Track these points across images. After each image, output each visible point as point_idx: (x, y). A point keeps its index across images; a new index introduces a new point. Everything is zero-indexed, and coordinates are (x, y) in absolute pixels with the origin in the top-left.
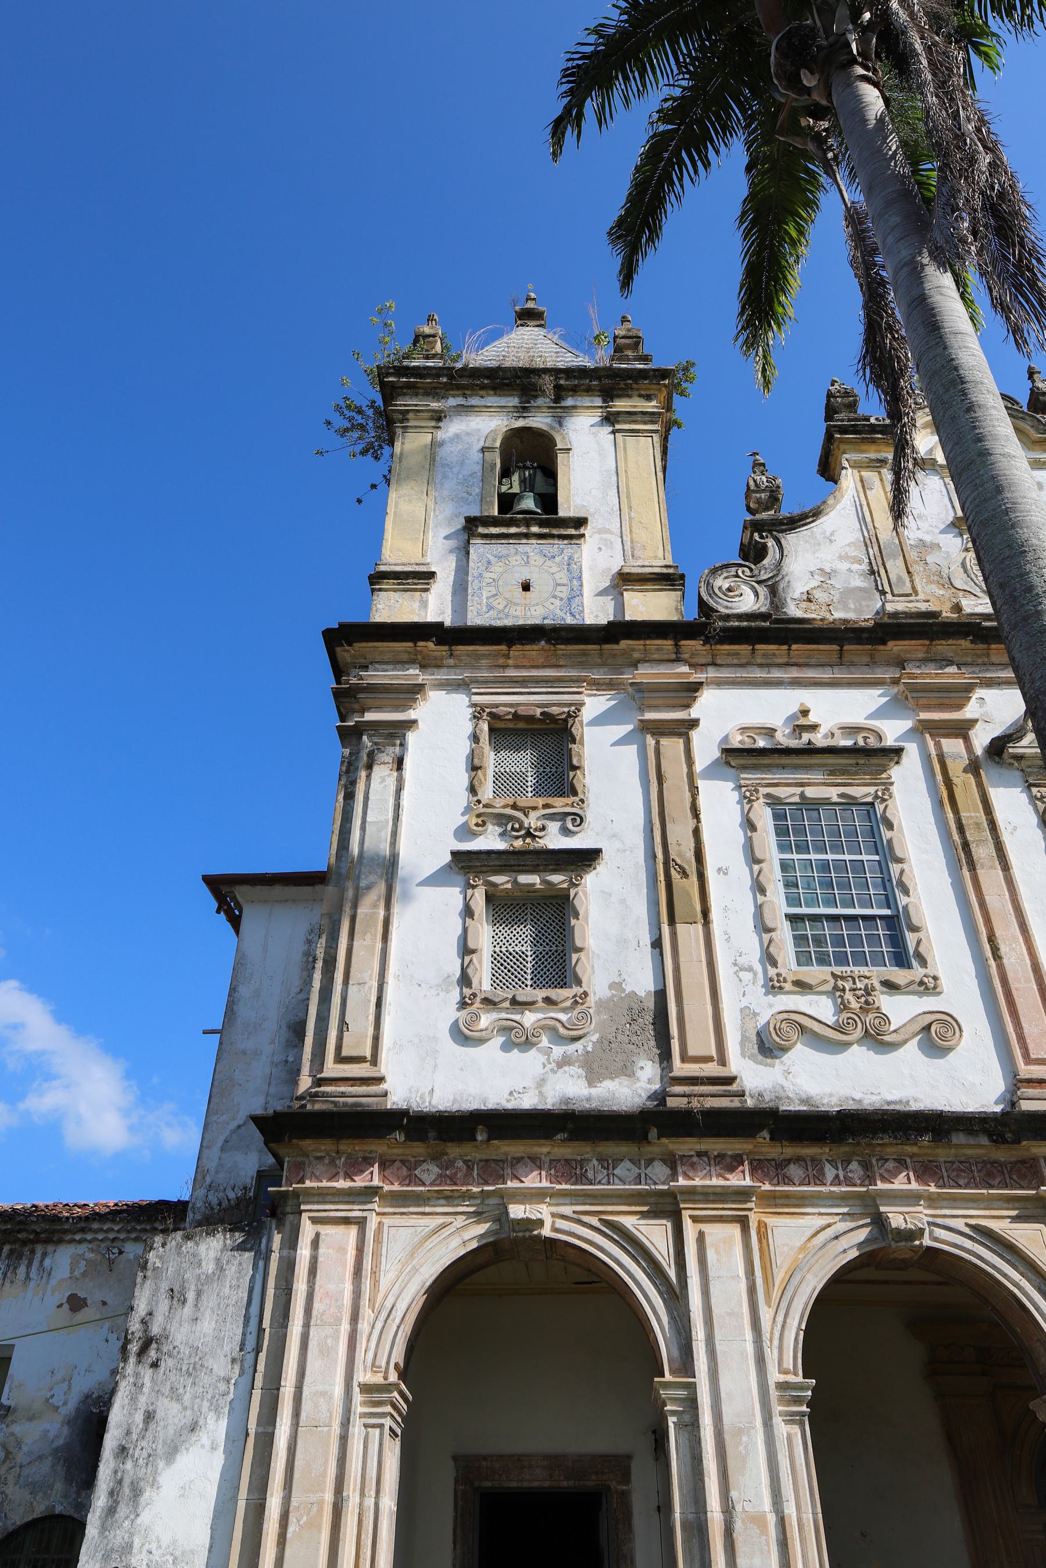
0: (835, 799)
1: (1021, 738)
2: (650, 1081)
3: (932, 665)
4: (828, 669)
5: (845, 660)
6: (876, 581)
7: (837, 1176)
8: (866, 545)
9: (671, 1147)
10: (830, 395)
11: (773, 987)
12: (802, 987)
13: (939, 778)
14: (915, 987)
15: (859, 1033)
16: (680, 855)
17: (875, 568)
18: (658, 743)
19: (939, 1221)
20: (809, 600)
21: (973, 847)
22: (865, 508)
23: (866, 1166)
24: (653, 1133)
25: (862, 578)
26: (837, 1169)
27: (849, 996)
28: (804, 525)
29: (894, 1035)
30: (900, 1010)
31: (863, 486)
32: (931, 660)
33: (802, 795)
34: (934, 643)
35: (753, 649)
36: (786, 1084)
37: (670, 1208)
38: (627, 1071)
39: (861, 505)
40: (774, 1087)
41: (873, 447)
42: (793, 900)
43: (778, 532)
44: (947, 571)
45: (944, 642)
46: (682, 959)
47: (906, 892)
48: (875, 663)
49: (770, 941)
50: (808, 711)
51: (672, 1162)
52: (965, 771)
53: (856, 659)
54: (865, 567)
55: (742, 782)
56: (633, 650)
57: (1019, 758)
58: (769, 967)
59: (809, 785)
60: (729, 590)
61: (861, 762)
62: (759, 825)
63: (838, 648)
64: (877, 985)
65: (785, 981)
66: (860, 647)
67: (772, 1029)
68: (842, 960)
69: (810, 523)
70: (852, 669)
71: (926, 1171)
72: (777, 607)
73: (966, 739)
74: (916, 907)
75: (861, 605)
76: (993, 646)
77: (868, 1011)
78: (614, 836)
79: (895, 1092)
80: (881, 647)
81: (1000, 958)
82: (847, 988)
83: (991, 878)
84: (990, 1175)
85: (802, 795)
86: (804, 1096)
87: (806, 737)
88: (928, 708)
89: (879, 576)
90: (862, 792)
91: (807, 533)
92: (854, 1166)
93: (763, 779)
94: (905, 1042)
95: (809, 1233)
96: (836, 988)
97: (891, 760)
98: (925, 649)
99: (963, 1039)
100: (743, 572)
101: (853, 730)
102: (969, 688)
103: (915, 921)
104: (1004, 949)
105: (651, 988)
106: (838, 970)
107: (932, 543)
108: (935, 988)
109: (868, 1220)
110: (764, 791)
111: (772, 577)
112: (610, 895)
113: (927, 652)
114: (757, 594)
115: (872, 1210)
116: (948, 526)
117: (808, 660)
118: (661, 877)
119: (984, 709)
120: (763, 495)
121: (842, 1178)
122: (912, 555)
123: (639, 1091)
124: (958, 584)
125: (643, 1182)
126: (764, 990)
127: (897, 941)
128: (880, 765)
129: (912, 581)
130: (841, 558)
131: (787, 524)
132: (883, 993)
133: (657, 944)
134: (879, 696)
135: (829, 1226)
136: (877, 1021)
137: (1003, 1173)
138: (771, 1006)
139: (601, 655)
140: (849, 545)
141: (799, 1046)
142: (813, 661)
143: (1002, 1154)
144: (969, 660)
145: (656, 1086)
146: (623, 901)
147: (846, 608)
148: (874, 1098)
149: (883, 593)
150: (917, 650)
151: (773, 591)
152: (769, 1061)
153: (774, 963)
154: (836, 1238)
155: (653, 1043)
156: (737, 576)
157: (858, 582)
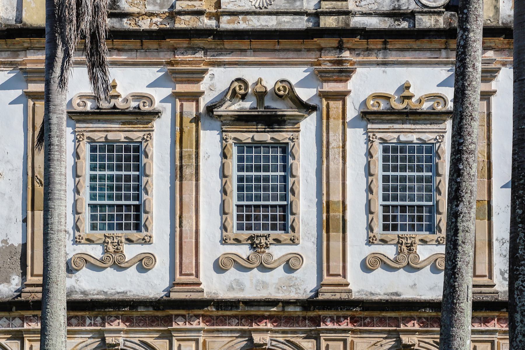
0: (123, 140)
1: (222, 105)
2: (17, 285)
3: (190, 52)
4: (134, 54)
5: (144, 47)
7: (91, 323)
9: (22, 313)
11: (76, 242)
12: (90, 241)
13: (178, 128)
14: (141, 241)
15: (111, 263)
16: (39, 173)
18: (34, 104)
19: (128, 339)
21: (184, 168)
23: (103, 319)
24: (14, 308)
26: (91, 320)
27: (110, 246)
29: (126, 264)
30: (130, 252)
33: (106, 138)
36: (76, 285)
37: (21, 336)
38: (7, 280)
40: (70, 287)
42: (93, 197)
46: (35, 229)
47: (147, 193)
48: (161, 48)
49: (79, 219)
50: (116, 86)
51: (23, 319)
52: (191, 122)
53: (150, 47)
55: (77, 130)
56: (24, 42)
57: (220, 116)
58: (76, 232)
59: (111, 131)
61: (139, 118)
62: (81, 156)
64: (123, 240)
65: (82, 239)
67: (72, 262)
68: (111, 227)
71: (127, 320)
73: (197, 102)
74: (150, 201)
77: (118, 252)
78: (8, 162)
79: (122, 288)
81: (182, 227)
82: (110, 242)
83: (189, 185)
84: (153, 321)
85: (106, 138)
86: (83, 291)
87: (113, 101)
88: (182, 82)
90: (137, 136)
92: (99, 319)
93: (87, 127)
94: (131, 266)
95: (75, 345)
96: (104, 242)
97: (155, 117)
98: (187, 42)
99: (156, 265)
101: (138, 97)
102: (205, 72)
103: (147, 209)
104: (184, 222)
105: (21, 242)
106: (107, 232)
108: (149, 241)
109: (100, 340)
110: (87, 134)
112: (4, 194)
113: (189, 44)
115: (102, 336)
117: (124, 47)
118: (30, 186)
119: (212, 82)
121: (92, 323)
123: (12, 289)
125: (11, 326)
126: (72, 242)
127: (138, 218)
128: (149, 119)
132: (126, 244)
133: (25, 221)
134: (157, 72)
135: (84, 342)
136: (119, 258)
137: (158, 320)
138: (74, 250)
139: (6, 43)
141: (84, 268)
142: (126, 47)
143: (159, 314)
144: (213, 47)
145: (19, 287)
146: (11, 198)
148: (113, 291)
150: (183, 43)
152: (70, 275)
153: (78, 230)
154: (86, 346)
155: (19, 268)
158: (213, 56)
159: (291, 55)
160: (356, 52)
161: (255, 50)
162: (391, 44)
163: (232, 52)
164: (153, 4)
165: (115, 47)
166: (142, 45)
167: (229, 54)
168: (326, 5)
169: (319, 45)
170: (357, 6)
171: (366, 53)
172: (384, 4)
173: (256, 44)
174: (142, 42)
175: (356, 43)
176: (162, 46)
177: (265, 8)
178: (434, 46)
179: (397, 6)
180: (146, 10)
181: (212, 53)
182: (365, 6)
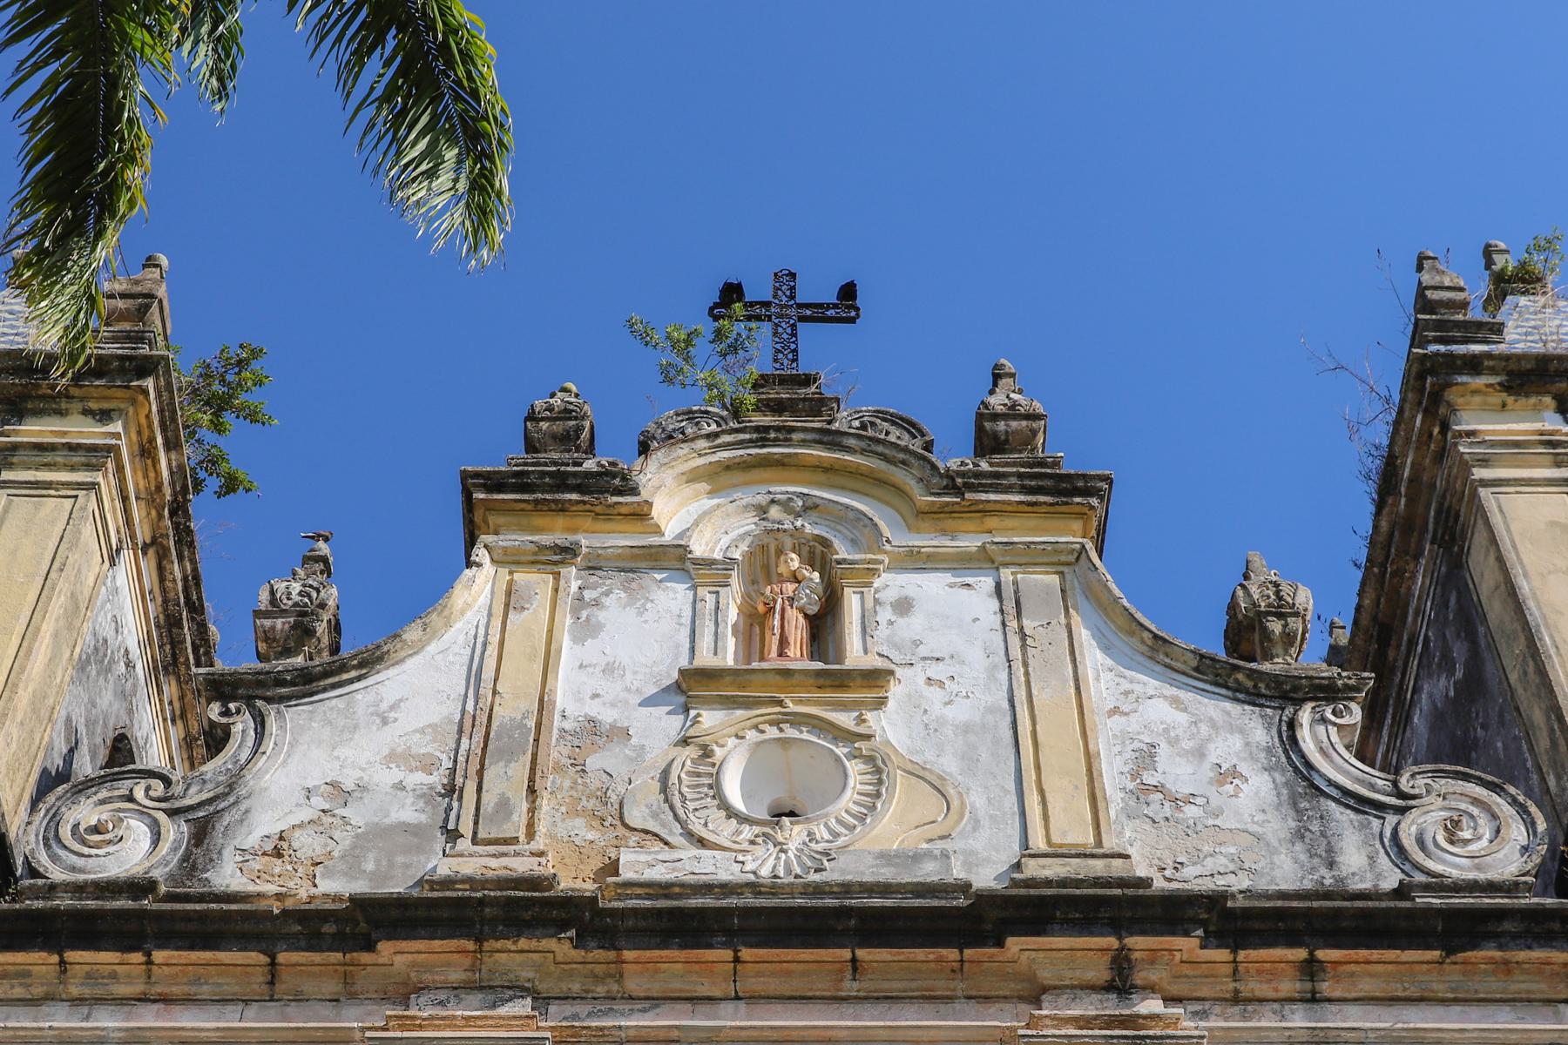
5: (279, 987)
6: (449, 809)
8: (460, 732)
10: (532, 417)
17: (459, 781)
20: (277, 853)
22: (492, 651)
25: (421, 804)
28: (334, 686)
31: (507, 605)
32: (481, 988)
34: (489, 945)
35: (62, 962)
39: (485, 645)
41: (561, 521)
43: (269, 700)
44: (621, 789)
45: (509, 944)
48: (353, 996)
53: (308, 987)
54: (438, 779)
60: (96, 830)
63: (264, 959)
66: (316, 957)
69: (351, 681)
70: (292, 1009)
72: (194, 868)
75: (391, 864)
76: (628, 955)
80: (365, 957)
89: (460, 798)
91: (340, 704)
100: (148, 789)
107: (613, 727)
111: (210, 801)
113: (472, 969)
114: (156, 838)
116: (667, 689)
117: (193, 989)
120: (279, 623)
122: (555, 751)
124: (636, 817)
129: (532, 811)
130: (392, 758)
131: (293, 683)
140: (422, 731)
142: (205, 991)
144: (576, 987)
147: (353, 870)
149: (453, 835)
150: (449, 964)
151: (201, 832)
156: (130, 798)
157: (408, 812)
158: (575, 1017)
159: (912, 1009)
160: (1191, 1008)
161: (753, 998)
162: (1337, 978)
163: (657, 1006)
164: (345, 874)
165: (158, 989)
166: (272, 983)
167: (644, 1011)
168: (1043, 867)
169: (1031, 978)
170: (1170, 880)
171: (1237, 1009)
172: (1278, 873)
173: (758, 974)
174: (273, 964)
175: (1186, 970)
176: (357, 988)
177: (797, 876)
178: (1524, 986)
179: (1328, 882)
180: (313, 891)
181: (569, 1009)
182: (1199, 881)
